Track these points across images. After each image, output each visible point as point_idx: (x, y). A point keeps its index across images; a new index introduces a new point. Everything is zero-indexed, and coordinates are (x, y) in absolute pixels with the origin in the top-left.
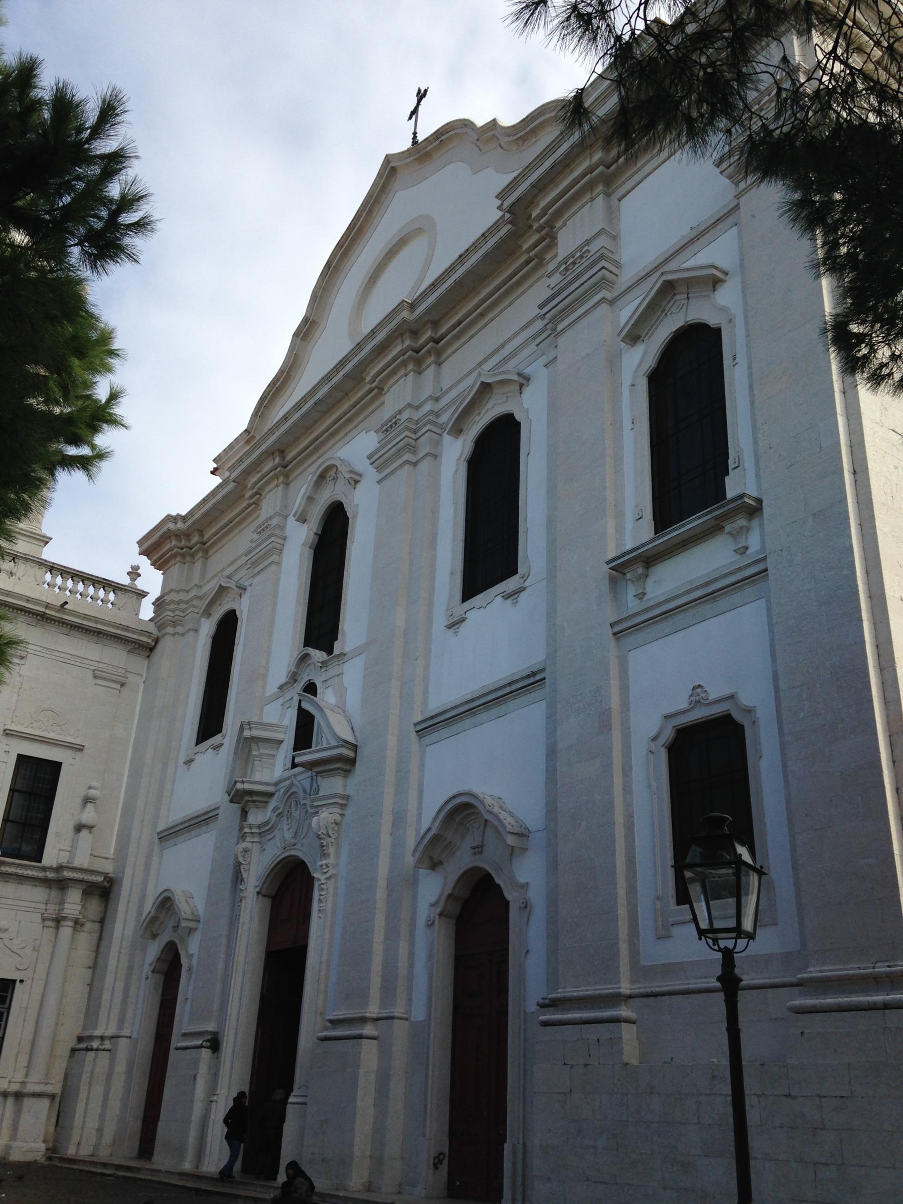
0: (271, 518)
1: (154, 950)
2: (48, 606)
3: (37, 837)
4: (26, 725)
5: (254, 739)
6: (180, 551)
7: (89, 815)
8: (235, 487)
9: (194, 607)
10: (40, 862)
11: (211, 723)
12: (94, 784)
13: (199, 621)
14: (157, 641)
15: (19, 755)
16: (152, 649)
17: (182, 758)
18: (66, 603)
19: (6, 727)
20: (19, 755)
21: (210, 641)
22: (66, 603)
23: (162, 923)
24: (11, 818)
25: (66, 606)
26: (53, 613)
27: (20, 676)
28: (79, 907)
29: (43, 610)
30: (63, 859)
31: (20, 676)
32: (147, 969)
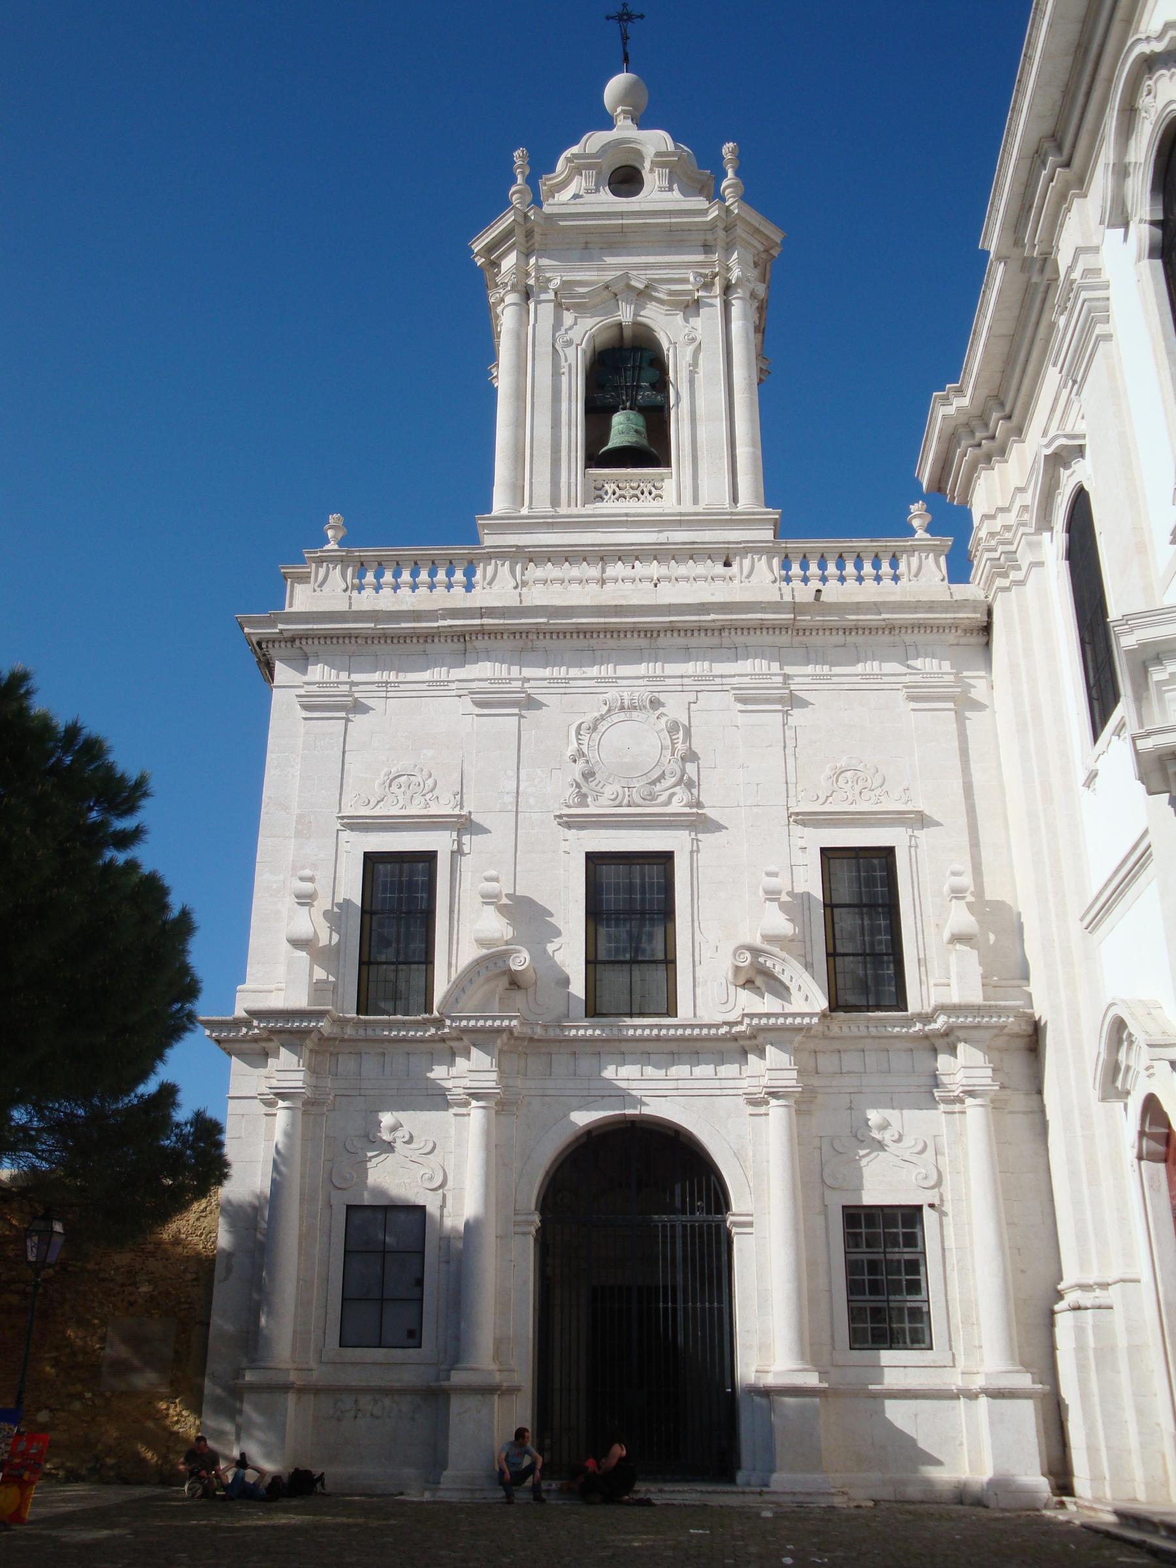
0: (1071, 269)
1: (1129, 1121)
3: (891, 972)
4: (821, 800)
5: (1144, 646)
6: (977, 451)
7: (960, 918)
8: (1005, 272)
9: (1024, 524)
10: (906, 1010)
11: (1102, 696)
12: (957, 867)
13: (1039, 545)
14: (990, 613)
15: (823, 850)
16: (987, 629)
17: (1082, 777)
19: (791, 810)
20: (823, 850)
21: (1064, 566)
23: (1128, 1068)
24: (840, 949)
27: (790, 728)
28: (989, 1072)
30: (936, 997)
31: (790, 728)
32: (1129, 1153)
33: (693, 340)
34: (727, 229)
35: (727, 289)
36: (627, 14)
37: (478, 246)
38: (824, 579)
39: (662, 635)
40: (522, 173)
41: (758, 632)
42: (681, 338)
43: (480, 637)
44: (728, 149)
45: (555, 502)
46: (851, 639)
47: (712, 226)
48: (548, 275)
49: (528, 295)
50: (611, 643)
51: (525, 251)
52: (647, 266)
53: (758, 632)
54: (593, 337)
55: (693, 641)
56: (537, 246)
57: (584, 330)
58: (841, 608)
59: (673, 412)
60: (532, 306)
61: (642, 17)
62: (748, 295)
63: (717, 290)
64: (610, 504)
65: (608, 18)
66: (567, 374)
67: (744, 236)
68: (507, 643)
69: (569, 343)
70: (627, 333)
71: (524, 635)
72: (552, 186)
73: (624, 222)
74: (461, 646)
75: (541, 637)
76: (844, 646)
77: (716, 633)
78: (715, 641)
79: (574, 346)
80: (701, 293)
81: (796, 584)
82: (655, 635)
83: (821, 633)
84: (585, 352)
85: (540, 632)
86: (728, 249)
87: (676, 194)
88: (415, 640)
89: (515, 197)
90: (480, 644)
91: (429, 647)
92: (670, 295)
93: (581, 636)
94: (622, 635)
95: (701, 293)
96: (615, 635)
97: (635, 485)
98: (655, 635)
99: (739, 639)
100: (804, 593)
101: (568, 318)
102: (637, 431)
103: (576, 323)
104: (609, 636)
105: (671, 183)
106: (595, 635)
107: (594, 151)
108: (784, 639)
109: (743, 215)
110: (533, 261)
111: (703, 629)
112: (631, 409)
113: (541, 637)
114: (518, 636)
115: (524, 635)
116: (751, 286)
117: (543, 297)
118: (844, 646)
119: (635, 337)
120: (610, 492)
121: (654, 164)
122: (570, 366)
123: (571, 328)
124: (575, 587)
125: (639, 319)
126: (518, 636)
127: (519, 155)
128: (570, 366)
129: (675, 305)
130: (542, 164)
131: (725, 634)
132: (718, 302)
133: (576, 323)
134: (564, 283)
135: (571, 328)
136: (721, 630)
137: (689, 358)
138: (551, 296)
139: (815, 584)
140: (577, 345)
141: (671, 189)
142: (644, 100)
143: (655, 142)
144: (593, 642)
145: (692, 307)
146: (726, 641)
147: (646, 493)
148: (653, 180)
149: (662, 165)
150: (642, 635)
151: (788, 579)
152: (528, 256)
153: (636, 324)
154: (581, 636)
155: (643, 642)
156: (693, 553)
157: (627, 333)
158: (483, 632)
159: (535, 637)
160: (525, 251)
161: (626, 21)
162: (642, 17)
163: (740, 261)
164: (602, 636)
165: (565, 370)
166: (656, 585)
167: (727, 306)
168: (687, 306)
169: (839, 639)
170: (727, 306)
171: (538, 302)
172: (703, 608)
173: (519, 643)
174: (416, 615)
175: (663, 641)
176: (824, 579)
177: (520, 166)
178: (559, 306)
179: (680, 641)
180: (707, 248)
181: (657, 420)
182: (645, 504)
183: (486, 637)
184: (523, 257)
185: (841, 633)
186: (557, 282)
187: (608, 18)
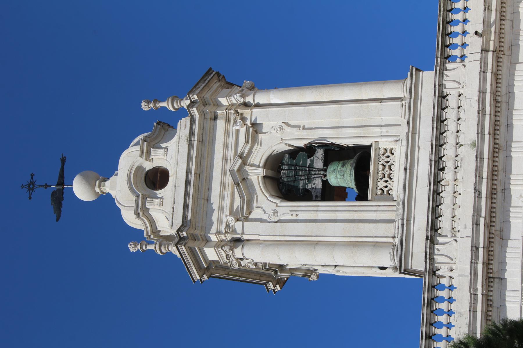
2: (485, 50)
18: (476, 33)
22: (476, 33)
25: (480, 31)
26: (492, 43)
29: (490, 54)
33: (281, 128)
34: (205, 104)
35: (246, 105)
36: (29, 185)
37: (197, 276)
38: (464, 33)
39: (497, 141)
40: (146, 245)
41: (500, 77)
42: (278, 135)
43: (491, 267)
44: (145, 107)
45: (392, 221)
46: (508, 16)
47: (203, 114)
48: (224, 226)
49: (237, 241)
50: (500, 177)
51: (204, 243)
52: (225, 159)
53: (500, 77)
54: (271, 195)
55: (503, 120)
56: (202, 234)
57: (265, 202)
58: (486, 22)
59: (331, 141)
60: (245, 237)
61: (32, 175)
62: (250, 92)
63: (246, 112)
64: (395, 184)
65: (30, 198)
66: (297, 213)
67: (210, 93)
68: (496, 248)
69: (275, 212)
70: (270, 173)
71: (492, 236)
72: (152, 231)
73: (193, 172)
74: (496, 280)
75: (493, 224)
76: (512, 21)
77: (499, 105)
78: (504, 106)
79: (277, 208)
80: (248, 122)
81: (466, 52)
82: (497, 146)
83: (503, 36)
84: (281, 201)
85: (490, 225)
86: (219, 105)
87: (172, 144)
88: (490, 313)
89: (164, 251)
90: (495, 267)
91: (495, 304)
92: (248, 142)
93: (495, 196)
94: (496, 168)
95: (248, 122)
96: (496, 173)
97: (381, 167)
98: (497, 146)
99: (504, 90)
100: (475, 44)
101: (256, 213)
102: (343, 166)
103: (261, 208)
104: (496, 178)
105: (162, 148)
106: (495, 187)
107: (134, 198)
108: (505, 61)
109: (198, 92)
110: (213, 238)
111: (495, 114)
112: (325, 170)
113: (493, 224)
114: (492, 240)
115: (492, 236)
116: (246, 90)
117: (239, 231)
118: (512, 21)
119: (272, 170)
120: (386, 184)
121: (148, 158)
122: (291, 211)
123: (264, 211)
124: (459, 200)
125: (261, 165)
126: (492, 240)
127: (132, 248)
128: (291, 211)
129: (255, 140)
130: (137, 235)
131: (499, 99)
132: (256, 112)
133: (261, 208)
134: (231, 214)
135: (264, 211)
136: (496, 101)
137: (294, 130)
138: (240, 223)
139: (467, 40)
140: (277, 206)
141: (166, 148)
142: (92, 174)
143: (130, 159)
144: (499, 189)
145: (256, 127)
146: (504, 99)
147: (388, 159)
148: (159, 159)
149: (148, 153)
150: (496, 155)
151: (463, 57)
152: (207, 241)
153: (265, 166)
154: (495, 196)
155: (501, 155)
156: (439, 121)
157: (270, 173)
158: (487, 264)
159: (494, 228)
160: (204, 243)
161: (34, 186)
162: (32, 175)
163: (229, 96)
164: (495, 182)
165: (294, 213)
166: (462, 145)
167: (258, 105)
168: (256, 132)
169: (507, 24)
170: (258, 105)
171: (243, 233)
172: (481, 111)
173: (497, 240)
174: (473, 311)
175: (502, 141)
176: (464, 33)
177: (141, 247)
178: (247, 219)
179: (502, 129)
180: (215, 118)
181: (335, 153)
182: (397, 160)
183: (492, 262)
184: (208, 244)
185: (503, 22)
186: (231, 220)
187: (30, 198)
